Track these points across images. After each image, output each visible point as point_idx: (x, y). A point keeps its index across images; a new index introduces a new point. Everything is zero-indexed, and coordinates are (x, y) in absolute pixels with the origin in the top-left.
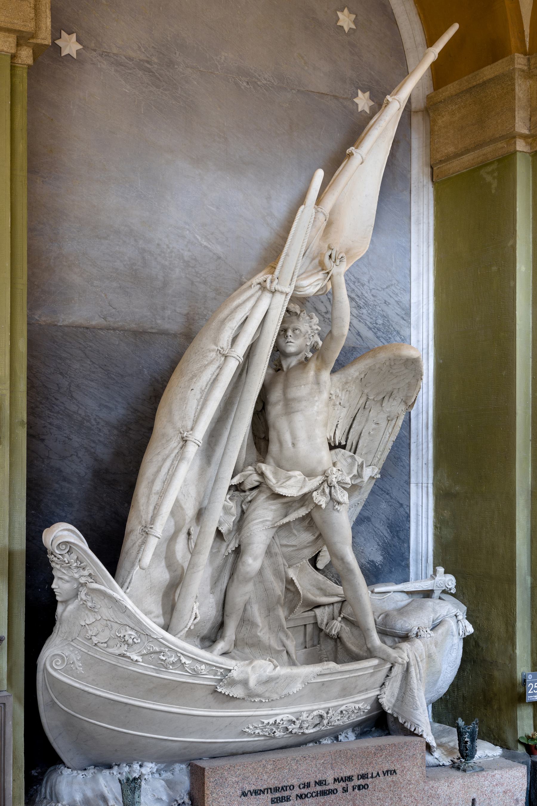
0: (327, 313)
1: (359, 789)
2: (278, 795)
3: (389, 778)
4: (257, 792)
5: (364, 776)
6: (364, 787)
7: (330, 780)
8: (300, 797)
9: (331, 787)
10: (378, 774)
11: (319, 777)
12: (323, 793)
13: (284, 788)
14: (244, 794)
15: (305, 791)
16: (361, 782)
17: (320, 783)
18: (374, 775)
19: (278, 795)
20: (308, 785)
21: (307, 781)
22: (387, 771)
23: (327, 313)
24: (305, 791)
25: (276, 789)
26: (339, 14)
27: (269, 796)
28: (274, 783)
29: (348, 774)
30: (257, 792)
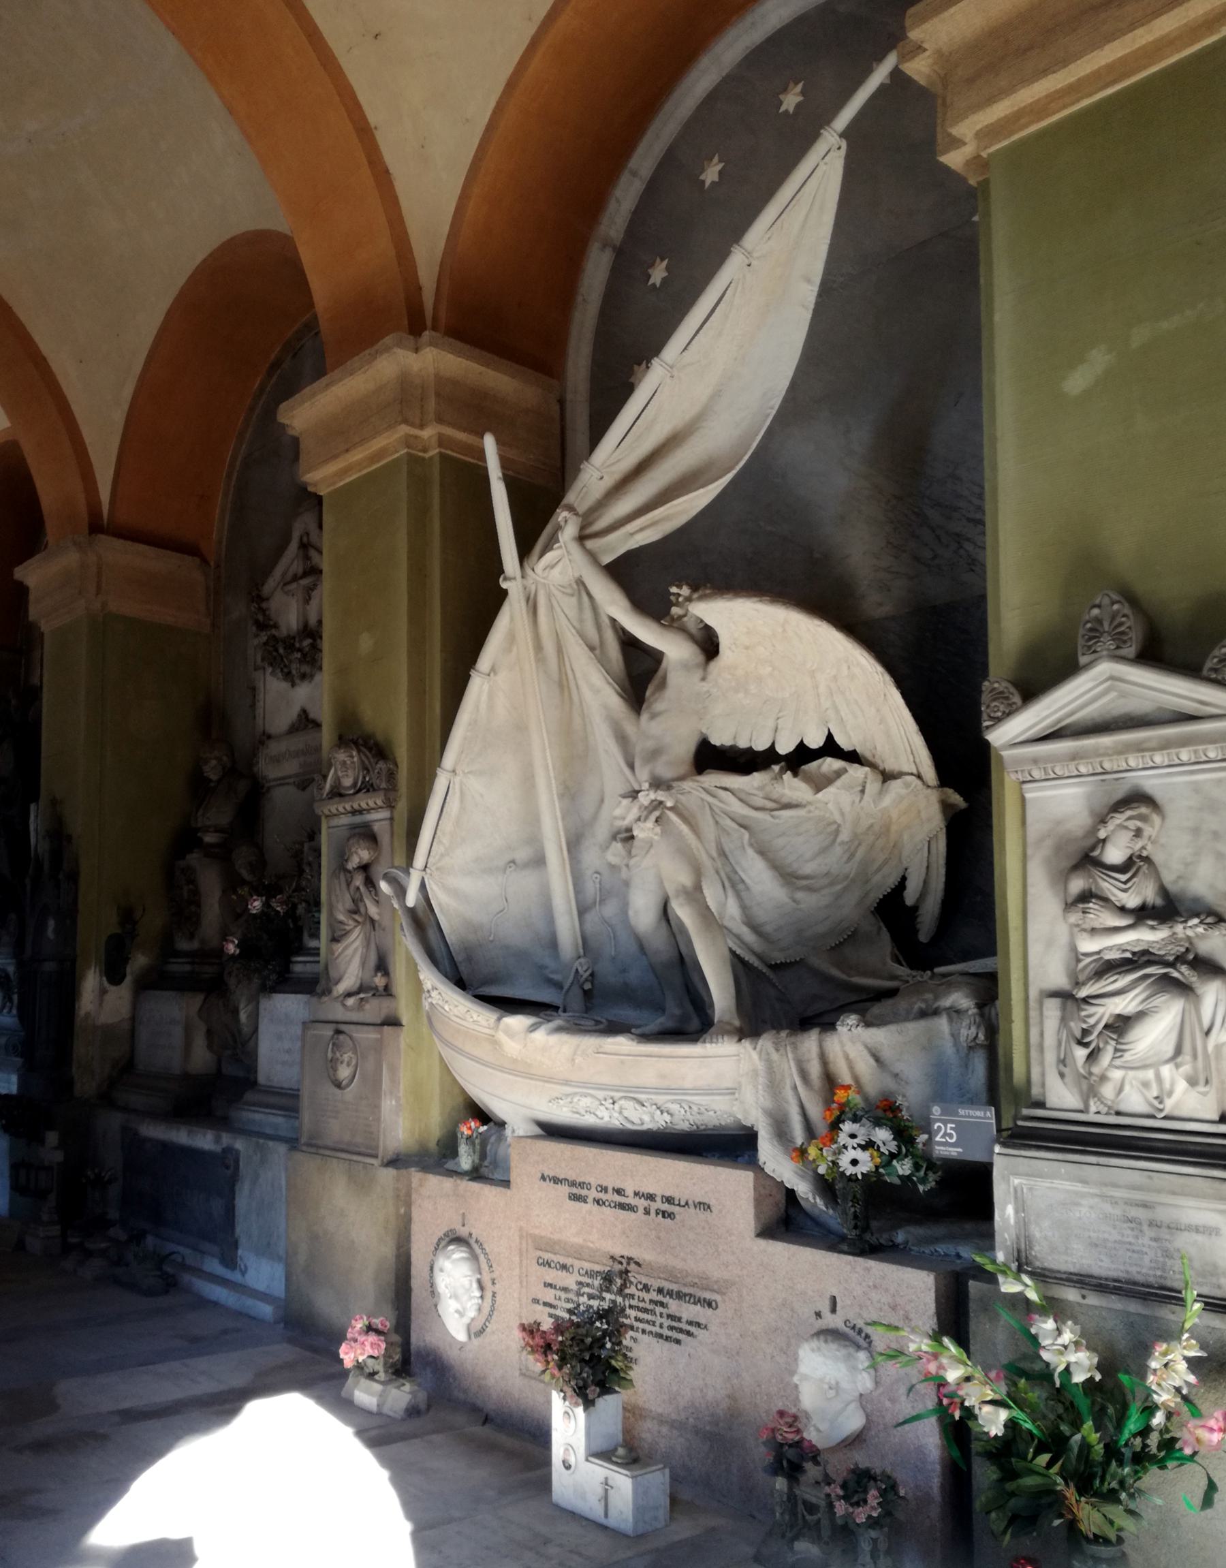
0: (935, 557)
1: (664, 1217)
2: (574, 1190)
3: (702, 1215)
4: (556, 1180)
5: (669, 1200)
6: (669, 1216)
7: (630, 1192)
8: (598, 1202)
9: (632, 1200)
10: (687, 1203)
11: (618, 1185)
12: (622, 1206)
13: (582, 1185)
14: (543, 1178)
15: (602, 1196)
16: (666, 1207)
17: (619, 1192)
18: (683, 1203)
19: (574, 1190)
20: (605, 1190)
21: (604, 1184)
22: (700, 1203)
23: (935, 557)
24: (602, 1196)
25: (573, 1184)
26: (707, 184)
27: (565, 1190)
28: (571, 1176)
29: (651, 1192)
30: (556, 1180)
